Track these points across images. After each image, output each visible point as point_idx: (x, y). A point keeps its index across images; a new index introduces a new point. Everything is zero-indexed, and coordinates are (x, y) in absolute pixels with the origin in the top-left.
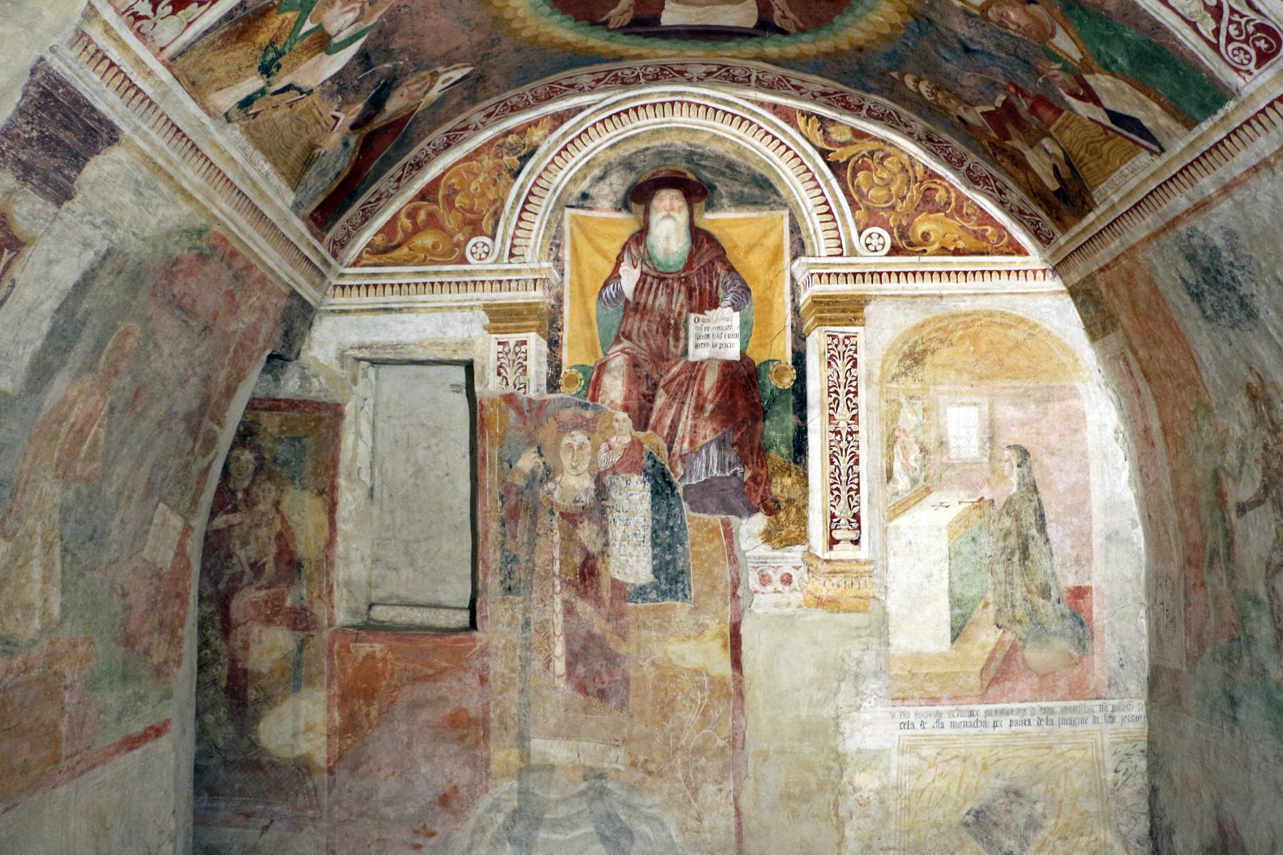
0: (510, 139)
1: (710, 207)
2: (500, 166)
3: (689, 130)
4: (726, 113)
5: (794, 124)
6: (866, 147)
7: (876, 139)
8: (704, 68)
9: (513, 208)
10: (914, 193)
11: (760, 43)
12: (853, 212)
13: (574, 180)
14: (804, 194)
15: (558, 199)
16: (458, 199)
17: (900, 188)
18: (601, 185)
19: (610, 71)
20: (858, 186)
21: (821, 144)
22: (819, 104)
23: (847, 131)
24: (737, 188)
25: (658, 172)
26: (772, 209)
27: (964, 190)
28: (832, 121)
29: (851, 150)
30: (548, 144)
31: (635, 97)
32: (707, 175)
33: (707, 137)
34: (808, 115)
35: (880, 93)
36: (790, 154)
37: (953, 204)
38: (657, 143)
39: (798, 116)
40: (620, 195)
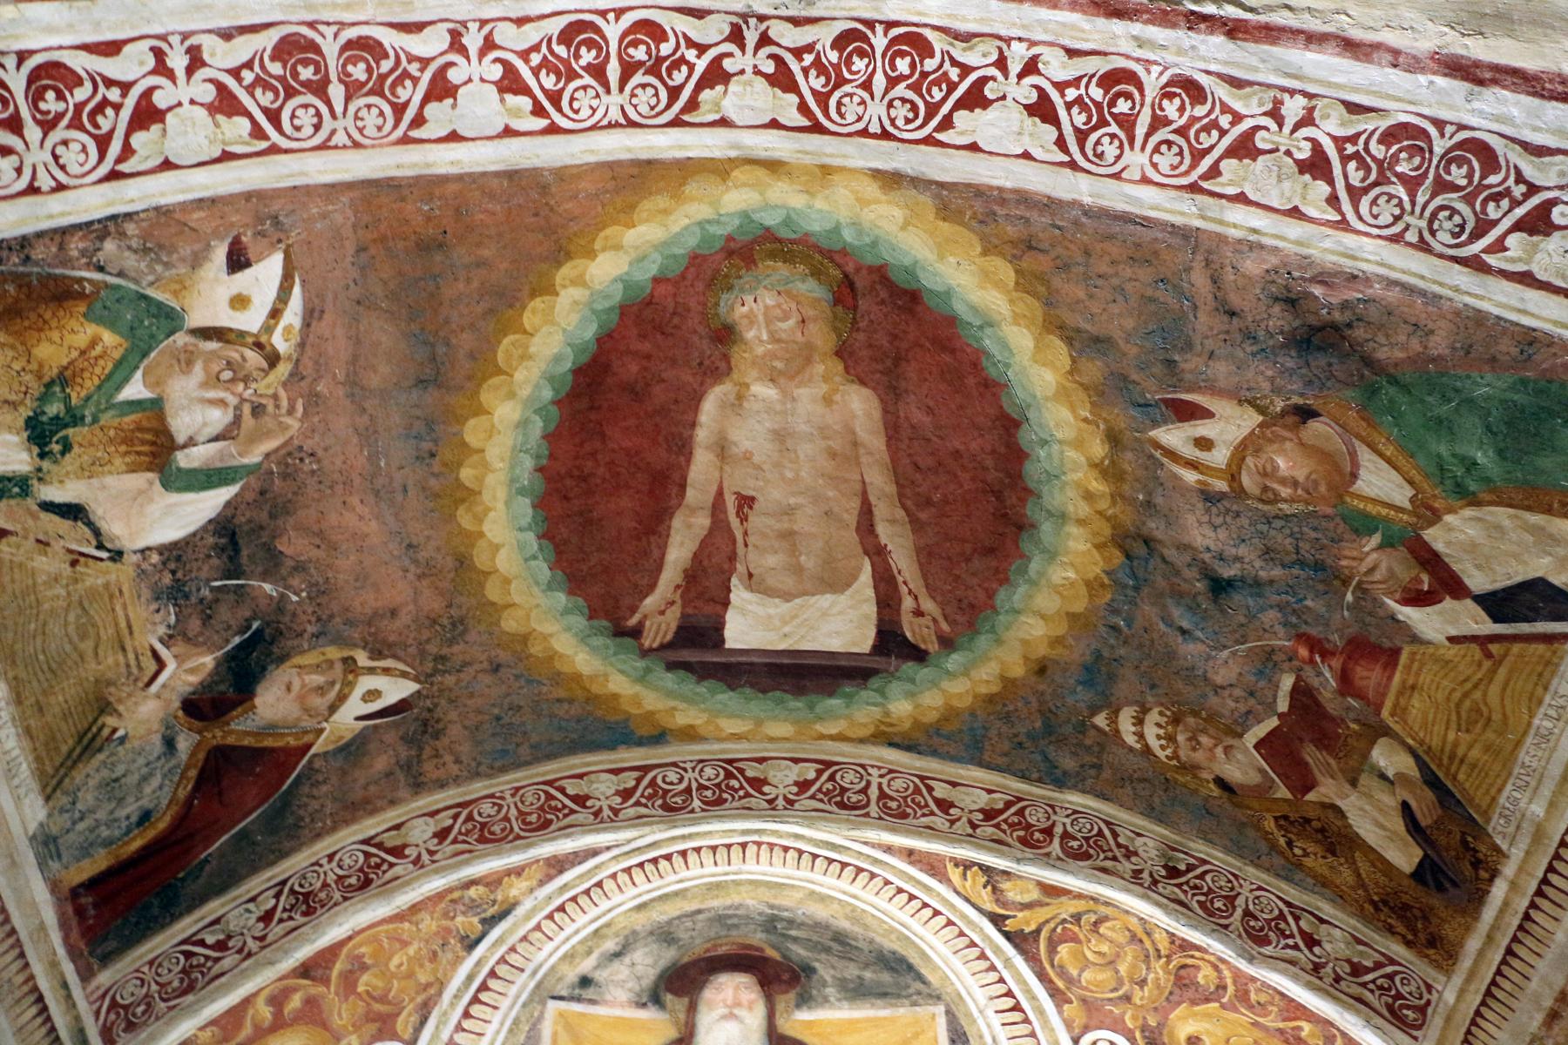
0: (473, 892)
1: (804, 1000)
2: (448, 931)
3: (768, 885)
4: (831, 861)
5: (943, 878)
6: (1068, 908)
7: (1080, 896)
8: (794, 773)
9: (457, 997)
10: (1159, 972)
11: (881, 692)
12: (1059, 1006)
13: (569, 957)
14: (970, 981)
15: (538, 986)
16: (365, 978)
17: (1133, 967)
18: (616, 965)
19: (645, 769)
20: (1061, 967)
21: (990, 906)
22: (979, 847)
23: (1031, 886)
24: (852, 971)
25: (715, 947)
26: (915, 1004)
27: (1243, 965)
28: (1006, 873)
29: (1041, 914)
30: (533, 902)
31: (683, 837)
32: (799, 952)
33: (799, 895)
34: (967, 865)
35: (1078, 784)
36: (941, 920)
37: (1231, 989)
38: (715, 903)
39: (950, 866)
40: (647, 982)
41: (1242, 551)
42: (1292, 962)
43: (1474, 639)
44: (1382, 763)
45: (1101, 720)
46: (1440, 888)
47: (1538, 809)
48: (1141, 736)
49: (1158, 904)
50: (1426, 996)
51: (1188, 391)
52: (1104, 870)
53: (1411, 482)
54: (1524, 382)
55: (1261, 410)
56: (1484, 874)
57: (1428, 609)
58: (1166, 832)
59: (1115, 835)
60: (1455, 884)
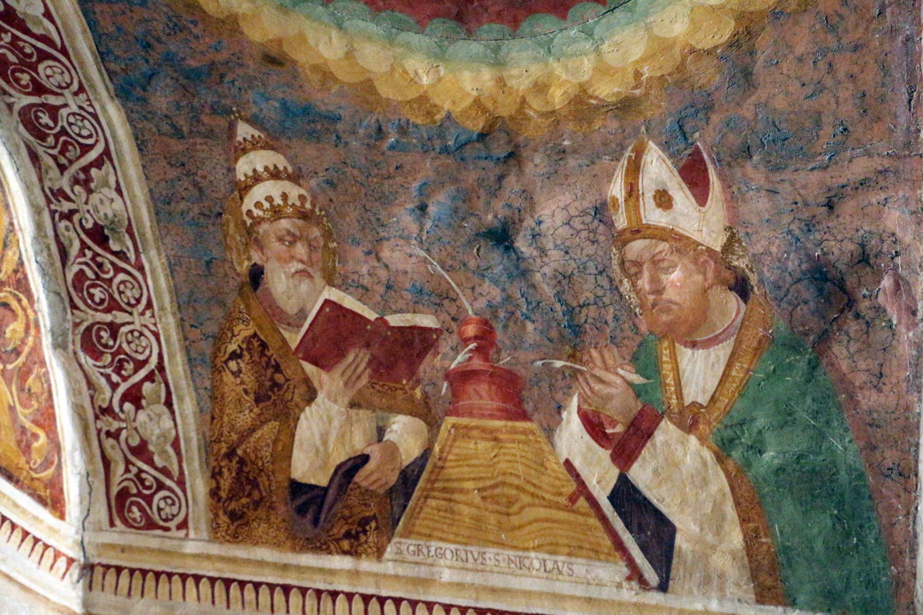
27: (47, 341)
37: (22, 359)
41: (555, 254)
42: (90, 385)
43: (581, 484)
44: (394, 427)
45: (244, 131)
46: (301, 511)
47: (447, 576)
48: (257, 179)
49: (39, 226)
50: (172, 524)
51: (720, 175)
52: (34, 157)
53: (713, 399)
54: (861, 476)
55: (728, 247)
56: (346, 544)
57: (587, 437)
58: (147, 223)
59: (98, 163)
60: (316, 522)
